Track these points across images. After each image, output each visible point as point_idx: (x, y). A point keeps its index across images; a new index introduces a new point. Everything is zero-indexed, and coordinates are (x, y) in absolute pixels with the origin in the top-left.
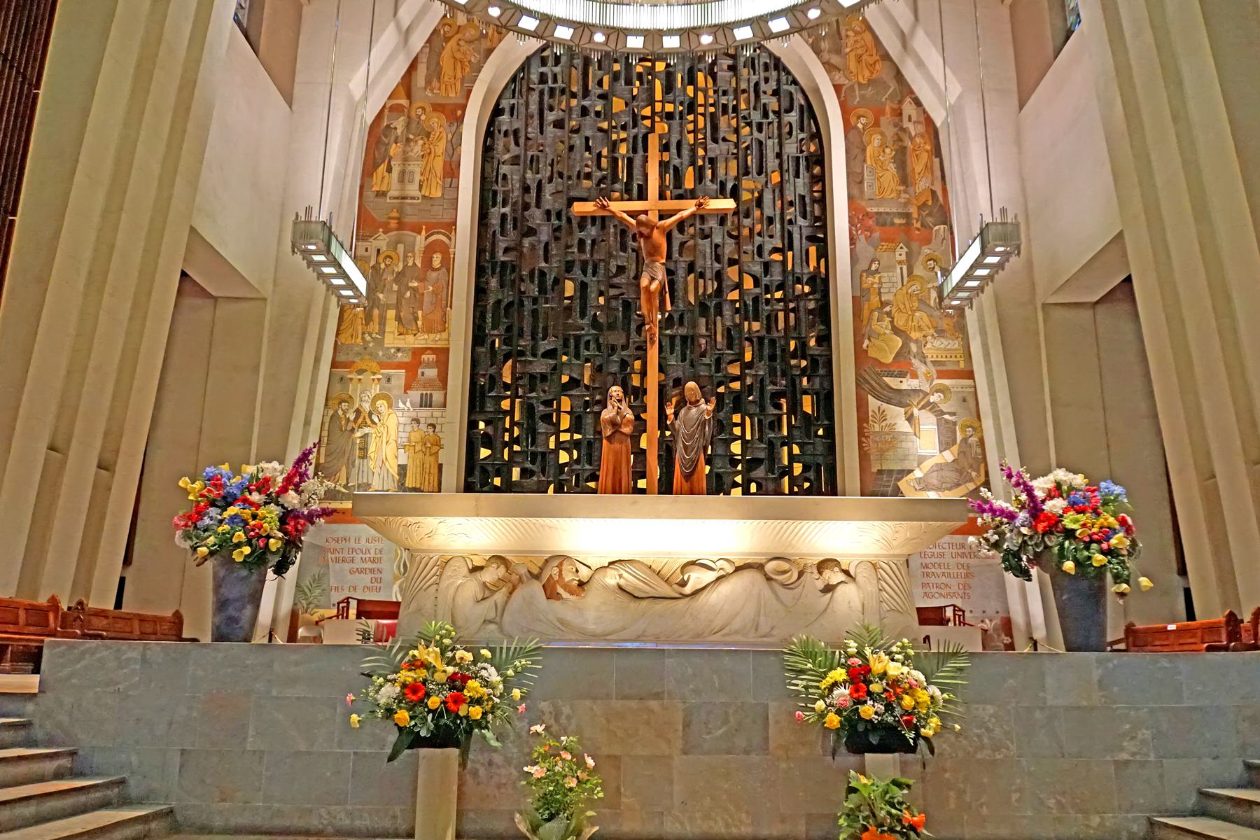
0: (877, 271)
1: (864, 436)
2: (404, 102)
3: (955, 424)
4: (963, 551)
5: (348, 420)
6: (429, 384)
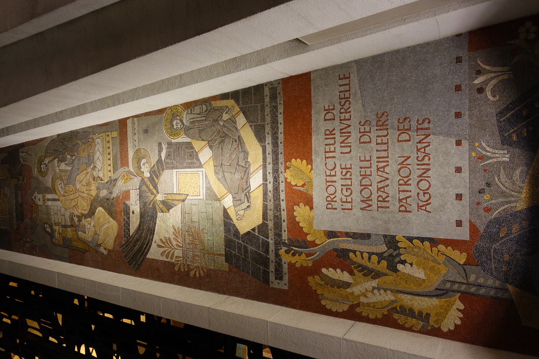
1: (188, 273)
3: (170, 144)
4: (337, 133)
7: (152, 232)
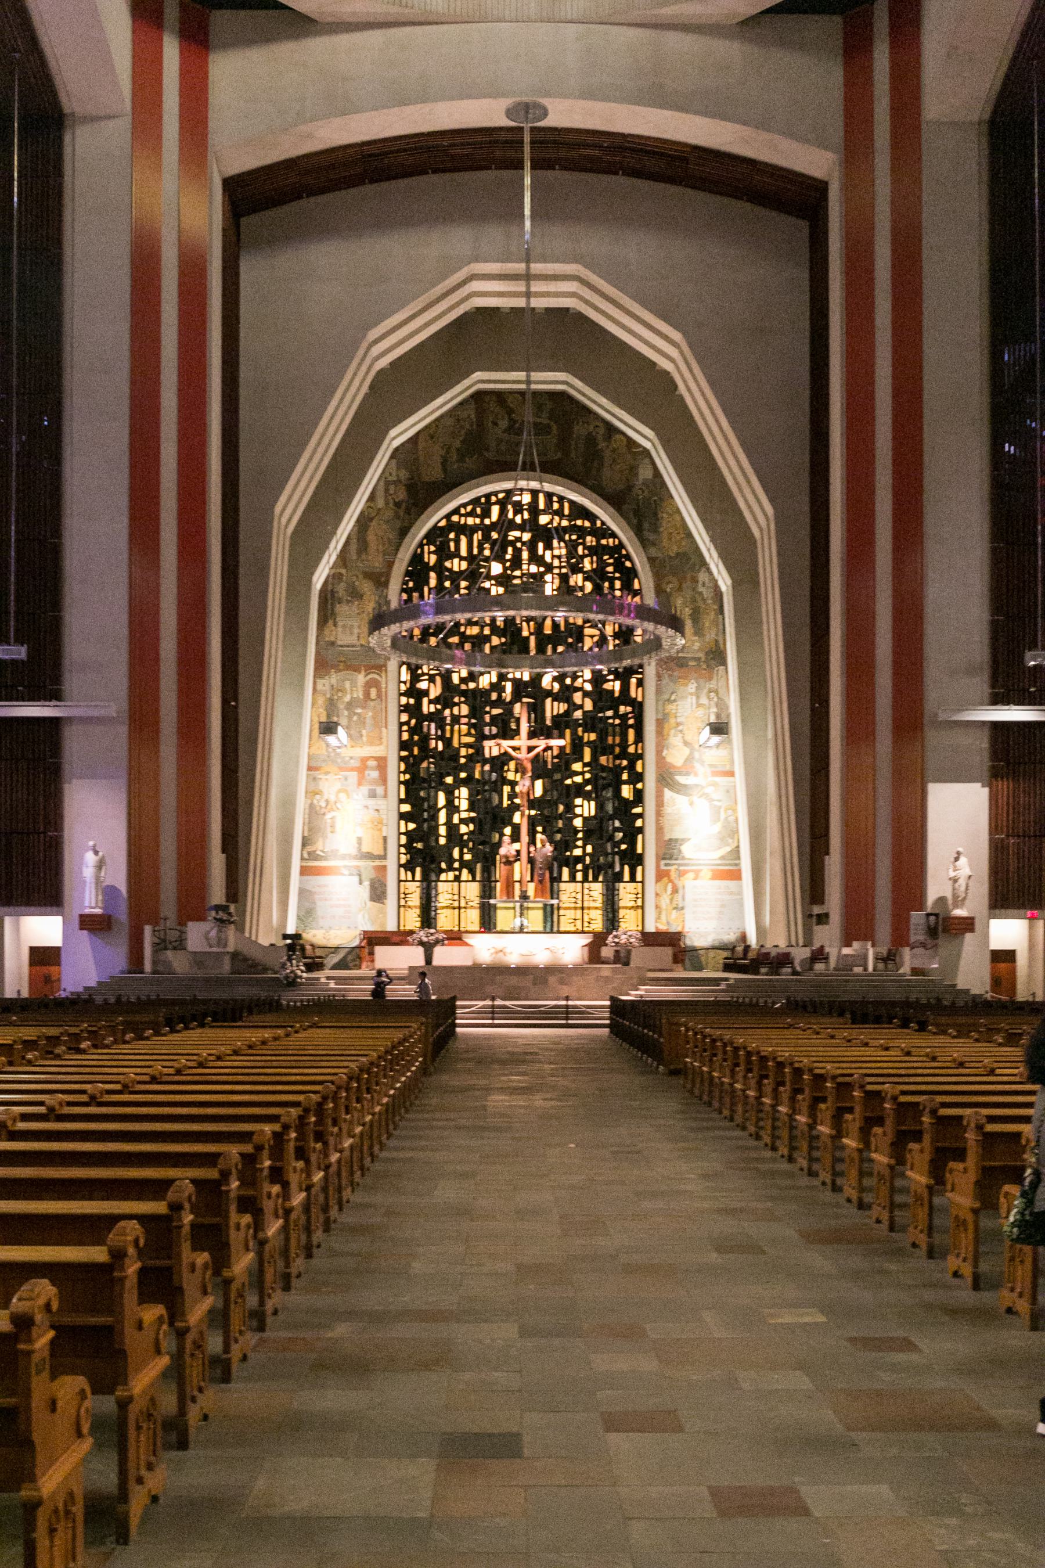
0: (675, 701)
2: (343, 571)
5: (321, 807)
6: (374, 782)
7: (678, 792)
